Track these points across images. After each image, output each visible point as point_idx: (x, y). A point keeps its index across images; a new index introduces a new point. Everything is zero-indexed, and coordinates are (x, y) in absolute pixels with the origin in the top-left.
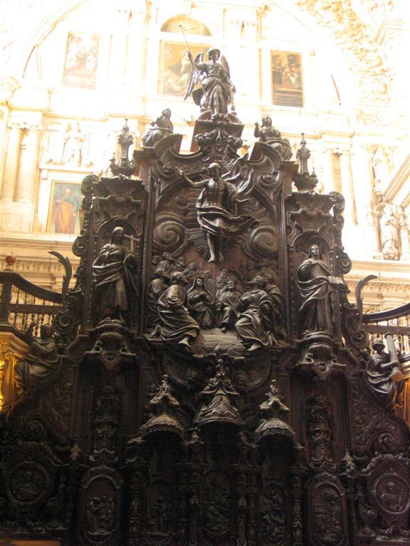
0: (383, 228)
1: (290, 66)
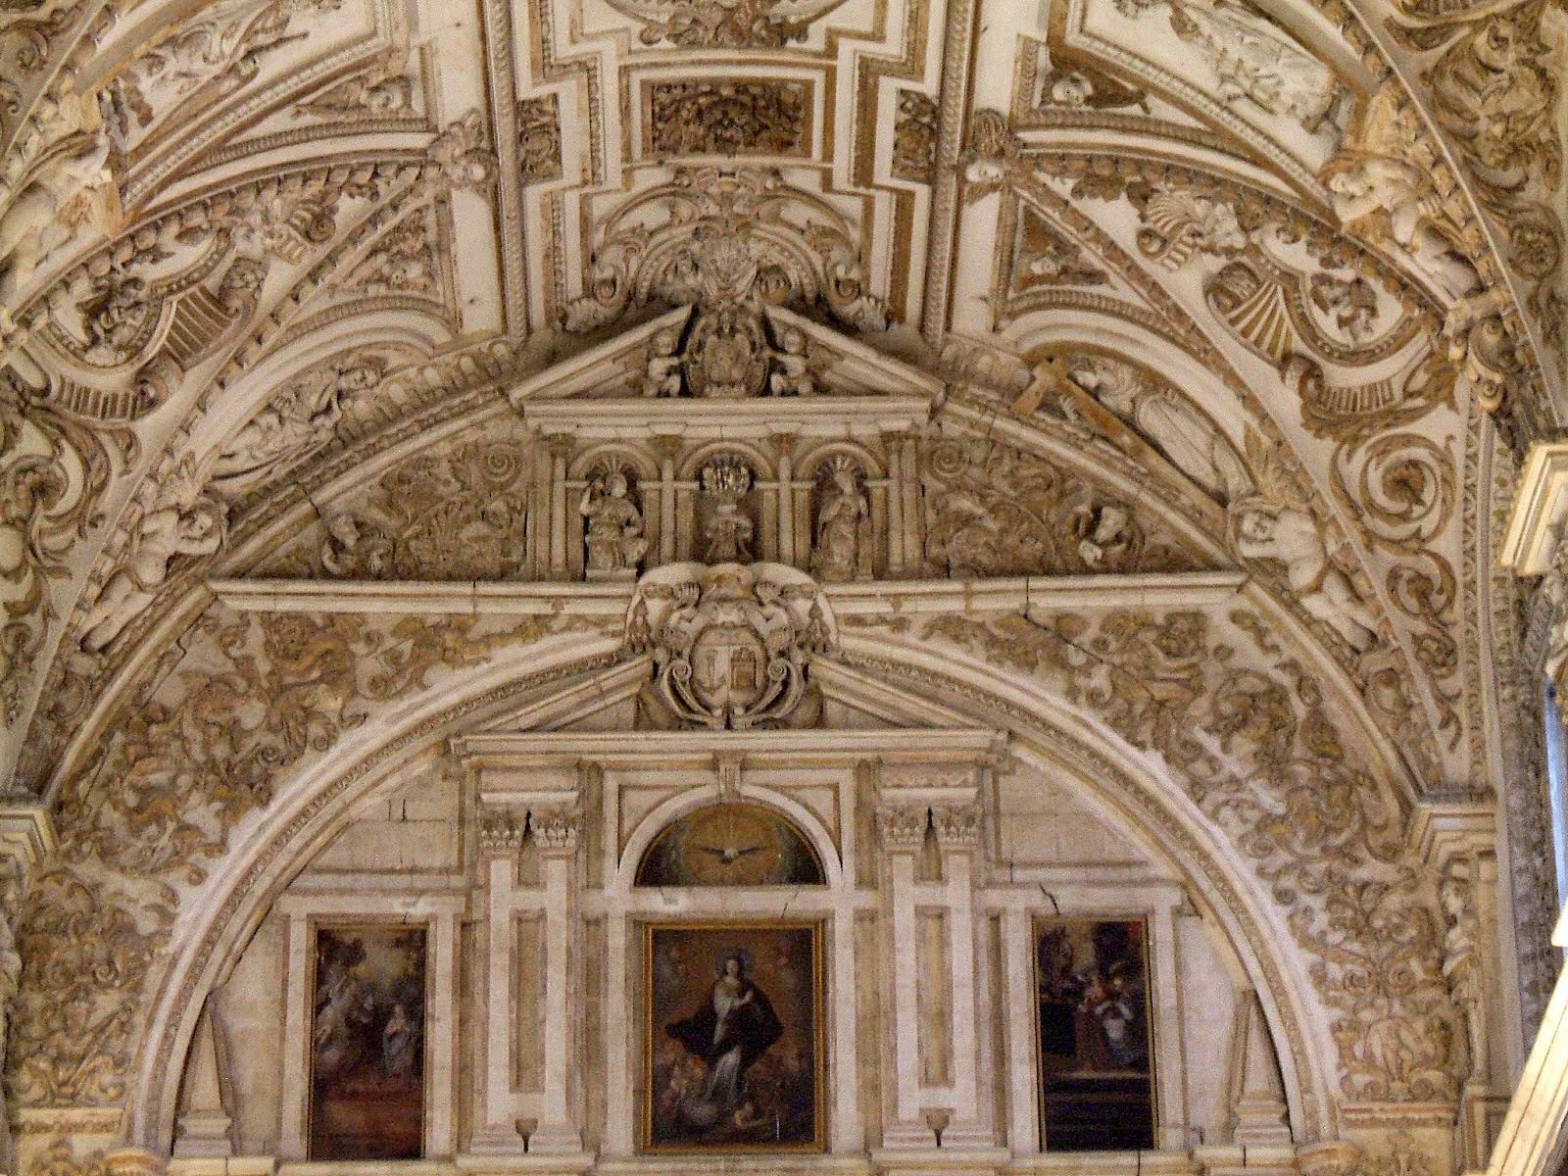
1: (1106, 977)
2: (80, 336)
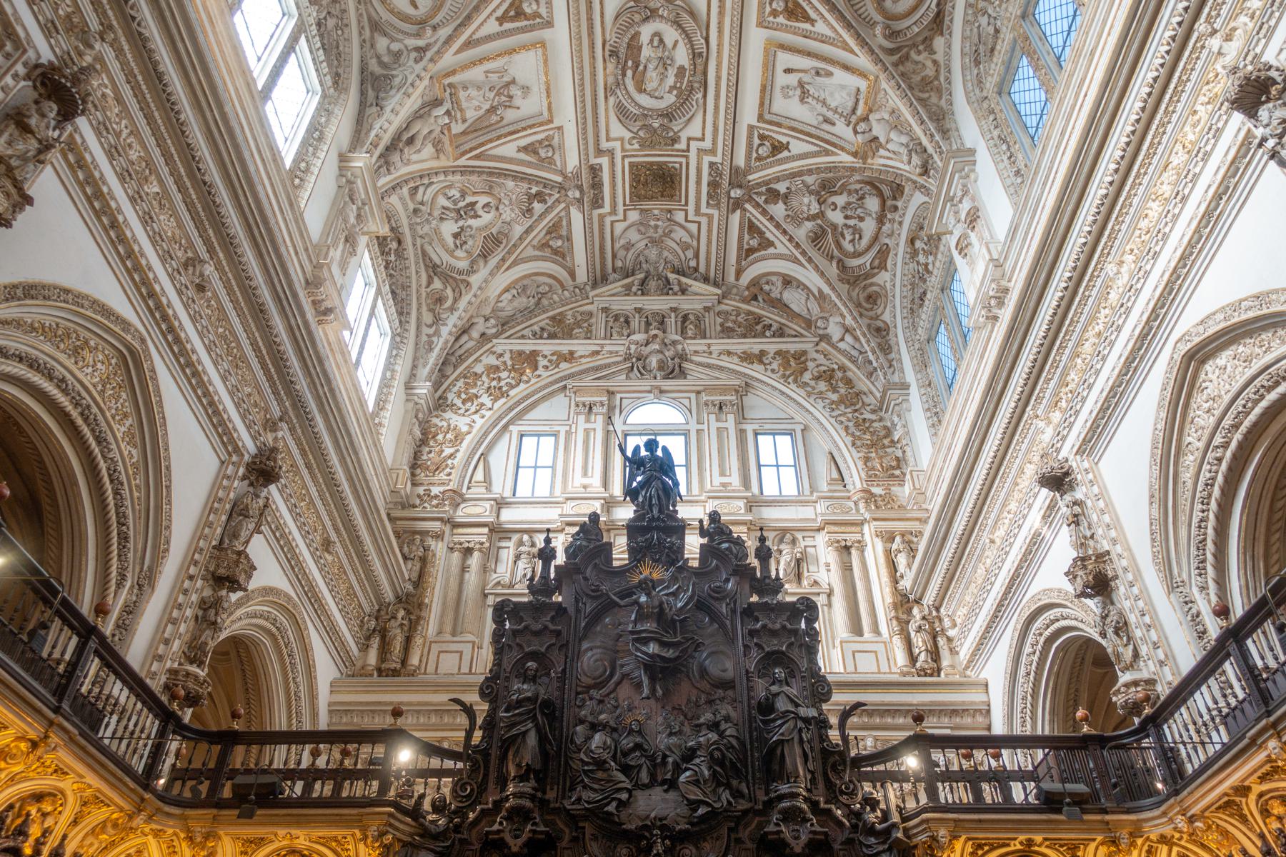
0: (913, 634)
2: (452, 246)
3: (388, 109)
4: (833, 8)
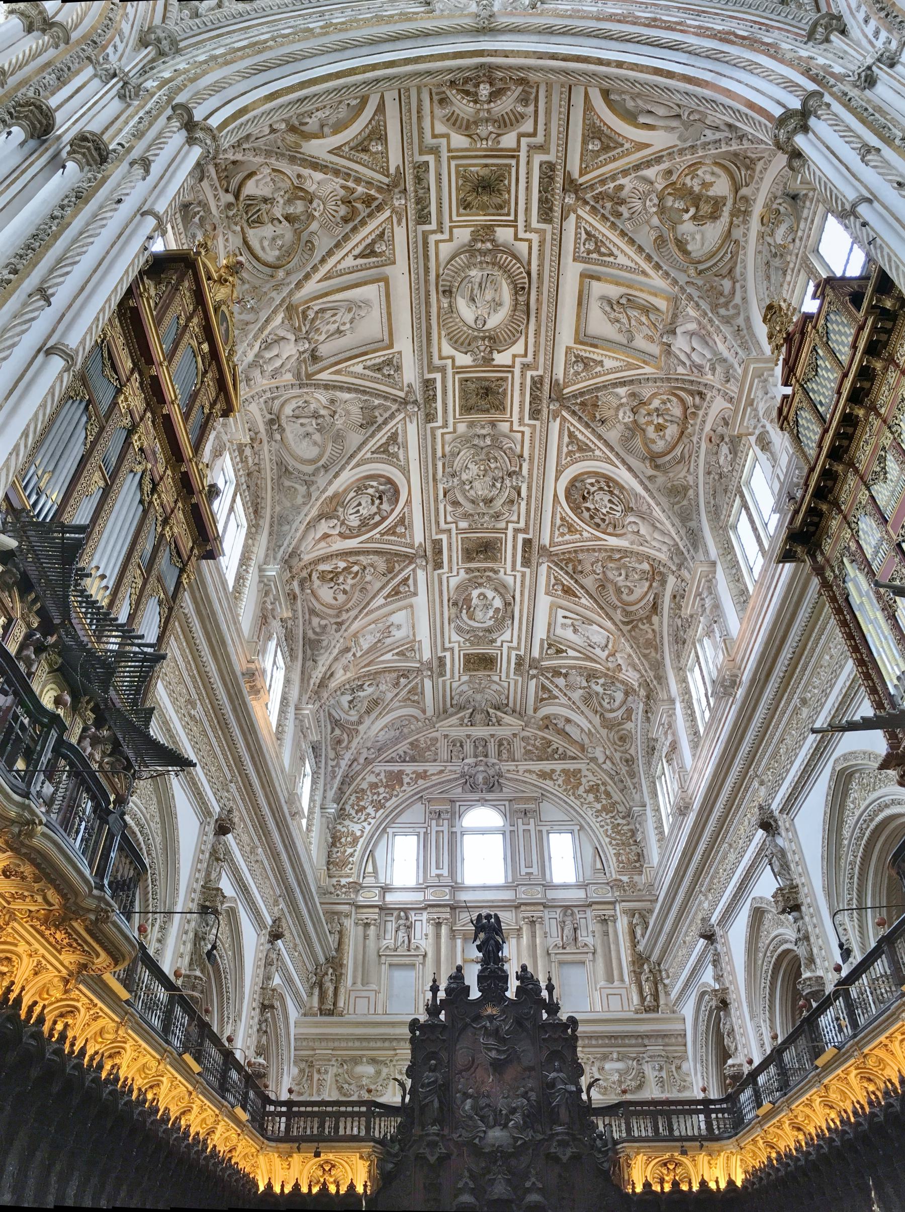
3: (320, 663)
4: (591, 596)
